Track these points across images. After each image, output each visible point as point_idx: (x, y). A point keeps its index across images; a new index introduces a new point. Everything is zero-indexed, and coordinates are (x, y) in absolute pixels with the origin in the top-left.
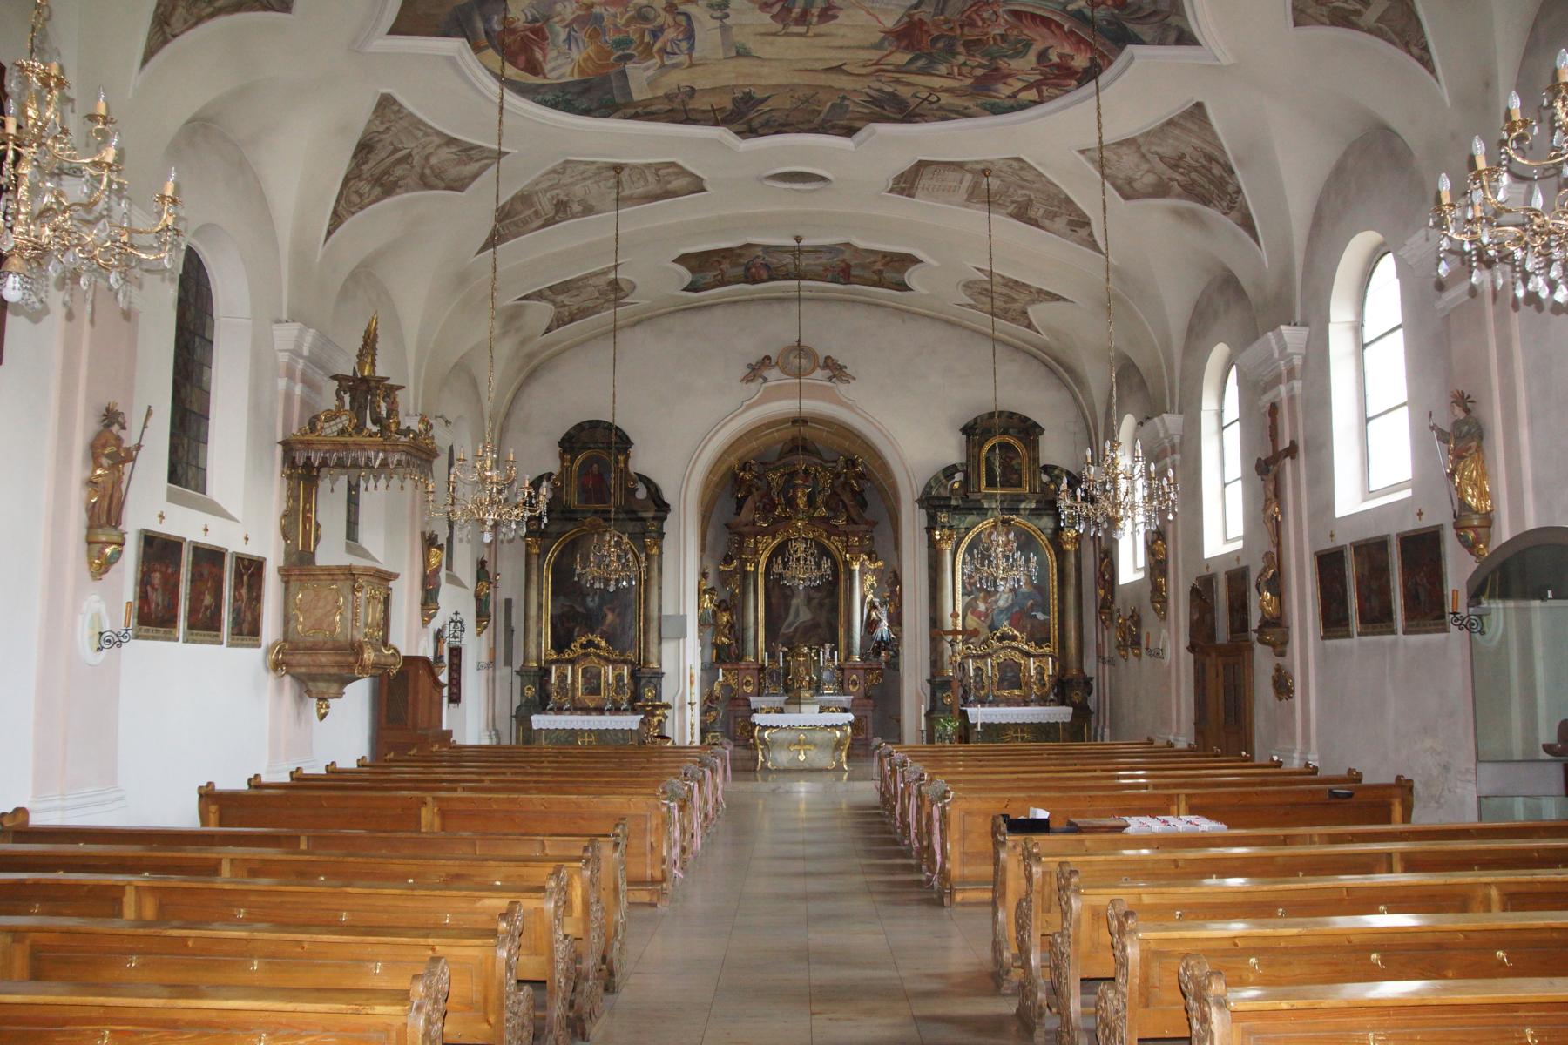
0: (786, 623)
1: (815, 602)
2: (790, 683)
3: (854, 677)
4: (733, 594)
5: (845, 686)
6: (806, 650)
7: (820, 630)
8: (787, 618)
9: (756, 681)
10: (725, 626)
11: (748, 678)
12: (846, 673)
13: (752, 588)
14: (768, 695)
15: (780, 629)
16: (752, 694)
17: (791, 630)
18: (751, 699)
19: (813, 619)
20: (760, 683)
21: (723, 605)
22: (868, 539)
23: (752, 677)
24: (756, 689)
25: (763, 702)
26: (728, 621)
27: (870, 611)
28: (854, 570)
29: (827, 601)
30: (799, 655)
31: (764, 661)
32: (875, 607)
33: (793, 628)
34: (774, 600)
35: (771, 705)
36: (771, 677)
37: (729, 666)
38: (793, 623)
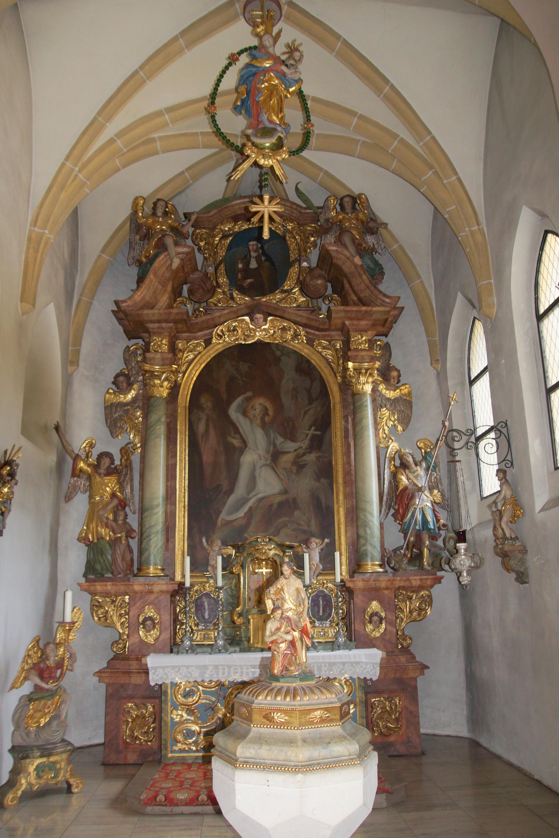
0: (232, 499)
1: (286, 460)
2: (239, 621)
3: (375, 606)
4: (125, 451)
5: (357, 626)
6: (272, 551)
7: (297, 513)
8: (231, 491)
9: (167, 617)
10: (108, 504)
11: (150, 612)
12: (358, 599)
13: (161, 430)
14: (194, 649)
15: (220, 512)
16: (157, 649)
17: (241, 513)
18: (152, 661)
19: (285, 492)
20: (176, 620)
21: (106, 462)
22: (381, 347)
23: (158, 612)
24: (166, 635)
25: (177, 668)
26: (113, 495)
27: (394, 476)
28: (364, 394)
29: (312, 457)
30: (258, 561)
31: (183, 576)
32: (404, 466)
33: (246, 508)
34: (207, 458)
35: (196, 676)
36: (199, 607)
37: (109, 587)
38: (244, 501)
